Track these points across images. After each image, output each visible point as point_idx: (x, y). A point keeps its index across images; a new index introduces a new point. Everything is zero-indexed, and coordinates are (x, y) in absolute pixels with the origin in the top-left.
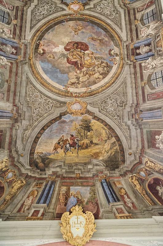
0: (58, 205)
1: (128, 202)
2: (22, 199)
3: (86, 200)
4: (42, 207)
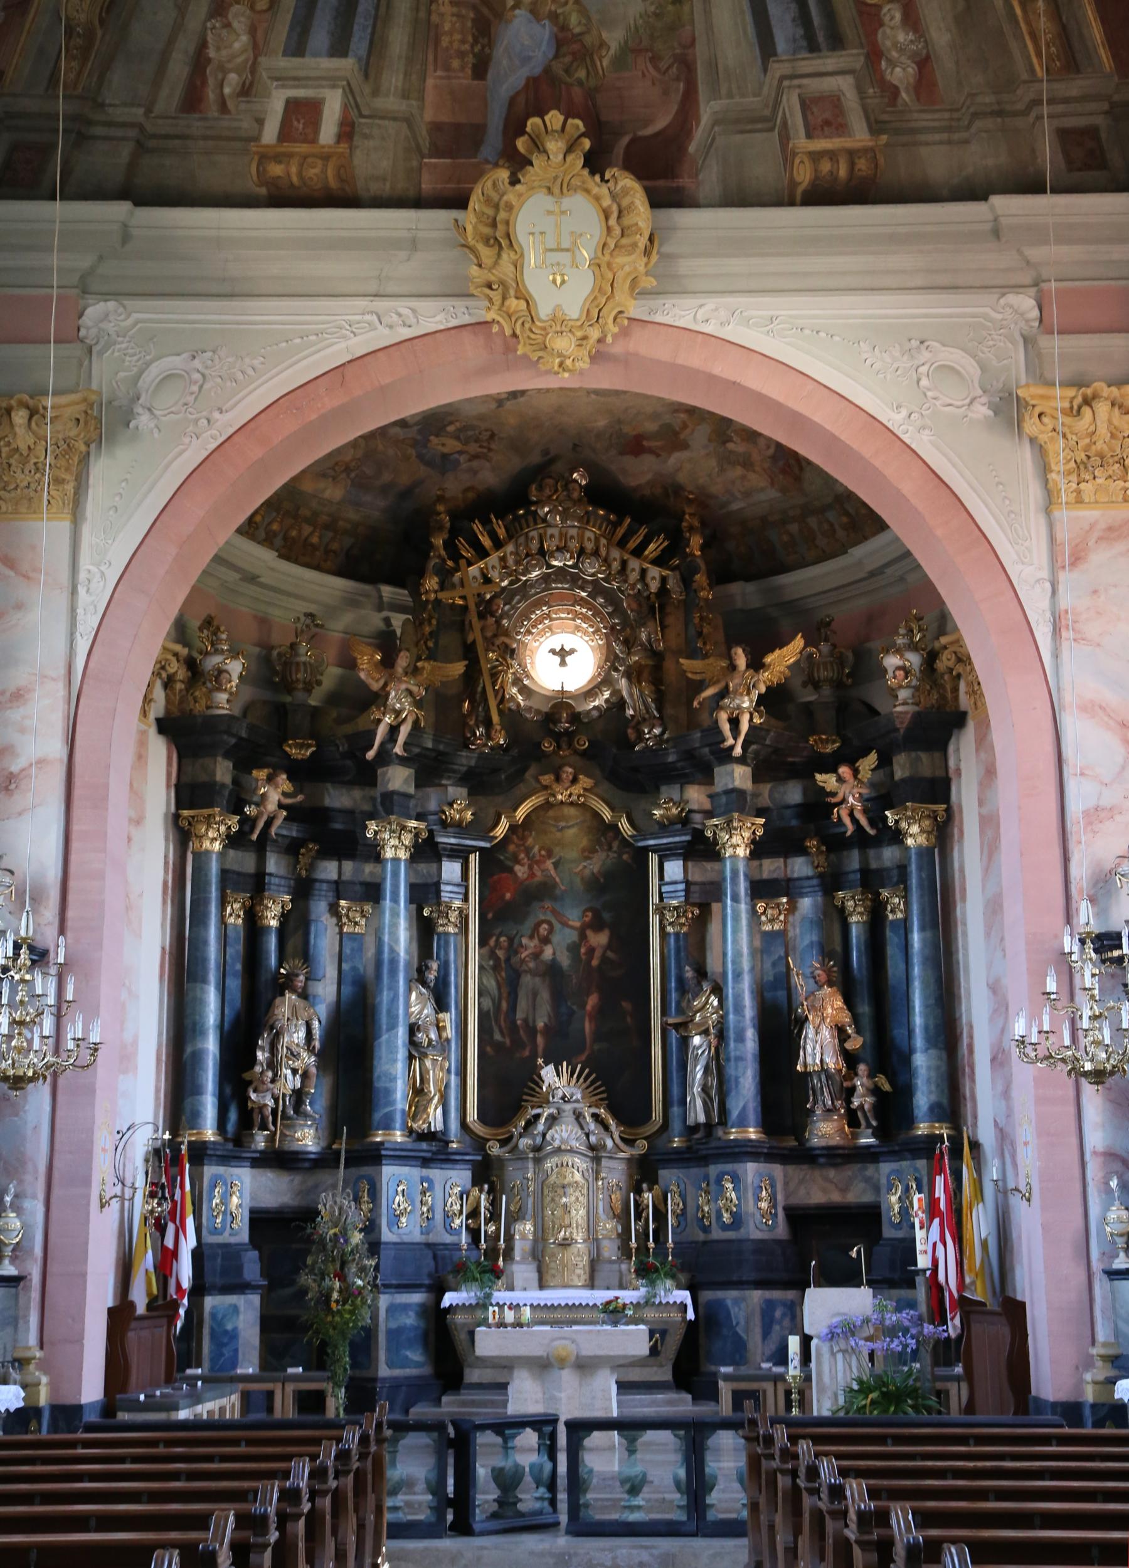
0: (431, 67)
1: (895, 54)
2: (178, 27)
3: (614, 38)
4: (332, 81)
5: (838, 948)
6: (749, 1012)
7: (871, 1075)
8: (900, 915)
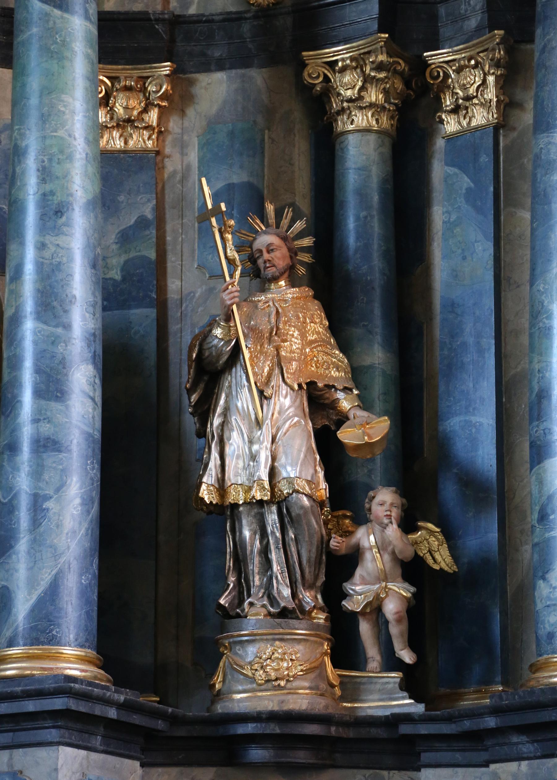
5: (305, 204)
6: (81, 319)
7: (408, 525)
8: (480, 117)
